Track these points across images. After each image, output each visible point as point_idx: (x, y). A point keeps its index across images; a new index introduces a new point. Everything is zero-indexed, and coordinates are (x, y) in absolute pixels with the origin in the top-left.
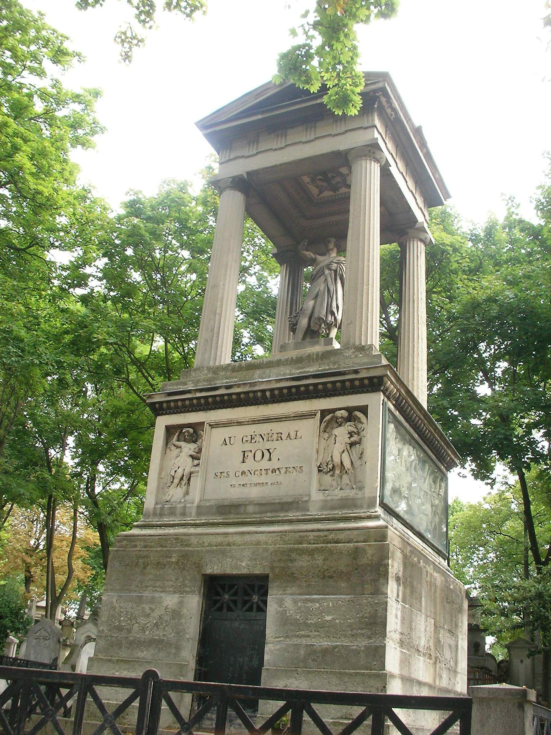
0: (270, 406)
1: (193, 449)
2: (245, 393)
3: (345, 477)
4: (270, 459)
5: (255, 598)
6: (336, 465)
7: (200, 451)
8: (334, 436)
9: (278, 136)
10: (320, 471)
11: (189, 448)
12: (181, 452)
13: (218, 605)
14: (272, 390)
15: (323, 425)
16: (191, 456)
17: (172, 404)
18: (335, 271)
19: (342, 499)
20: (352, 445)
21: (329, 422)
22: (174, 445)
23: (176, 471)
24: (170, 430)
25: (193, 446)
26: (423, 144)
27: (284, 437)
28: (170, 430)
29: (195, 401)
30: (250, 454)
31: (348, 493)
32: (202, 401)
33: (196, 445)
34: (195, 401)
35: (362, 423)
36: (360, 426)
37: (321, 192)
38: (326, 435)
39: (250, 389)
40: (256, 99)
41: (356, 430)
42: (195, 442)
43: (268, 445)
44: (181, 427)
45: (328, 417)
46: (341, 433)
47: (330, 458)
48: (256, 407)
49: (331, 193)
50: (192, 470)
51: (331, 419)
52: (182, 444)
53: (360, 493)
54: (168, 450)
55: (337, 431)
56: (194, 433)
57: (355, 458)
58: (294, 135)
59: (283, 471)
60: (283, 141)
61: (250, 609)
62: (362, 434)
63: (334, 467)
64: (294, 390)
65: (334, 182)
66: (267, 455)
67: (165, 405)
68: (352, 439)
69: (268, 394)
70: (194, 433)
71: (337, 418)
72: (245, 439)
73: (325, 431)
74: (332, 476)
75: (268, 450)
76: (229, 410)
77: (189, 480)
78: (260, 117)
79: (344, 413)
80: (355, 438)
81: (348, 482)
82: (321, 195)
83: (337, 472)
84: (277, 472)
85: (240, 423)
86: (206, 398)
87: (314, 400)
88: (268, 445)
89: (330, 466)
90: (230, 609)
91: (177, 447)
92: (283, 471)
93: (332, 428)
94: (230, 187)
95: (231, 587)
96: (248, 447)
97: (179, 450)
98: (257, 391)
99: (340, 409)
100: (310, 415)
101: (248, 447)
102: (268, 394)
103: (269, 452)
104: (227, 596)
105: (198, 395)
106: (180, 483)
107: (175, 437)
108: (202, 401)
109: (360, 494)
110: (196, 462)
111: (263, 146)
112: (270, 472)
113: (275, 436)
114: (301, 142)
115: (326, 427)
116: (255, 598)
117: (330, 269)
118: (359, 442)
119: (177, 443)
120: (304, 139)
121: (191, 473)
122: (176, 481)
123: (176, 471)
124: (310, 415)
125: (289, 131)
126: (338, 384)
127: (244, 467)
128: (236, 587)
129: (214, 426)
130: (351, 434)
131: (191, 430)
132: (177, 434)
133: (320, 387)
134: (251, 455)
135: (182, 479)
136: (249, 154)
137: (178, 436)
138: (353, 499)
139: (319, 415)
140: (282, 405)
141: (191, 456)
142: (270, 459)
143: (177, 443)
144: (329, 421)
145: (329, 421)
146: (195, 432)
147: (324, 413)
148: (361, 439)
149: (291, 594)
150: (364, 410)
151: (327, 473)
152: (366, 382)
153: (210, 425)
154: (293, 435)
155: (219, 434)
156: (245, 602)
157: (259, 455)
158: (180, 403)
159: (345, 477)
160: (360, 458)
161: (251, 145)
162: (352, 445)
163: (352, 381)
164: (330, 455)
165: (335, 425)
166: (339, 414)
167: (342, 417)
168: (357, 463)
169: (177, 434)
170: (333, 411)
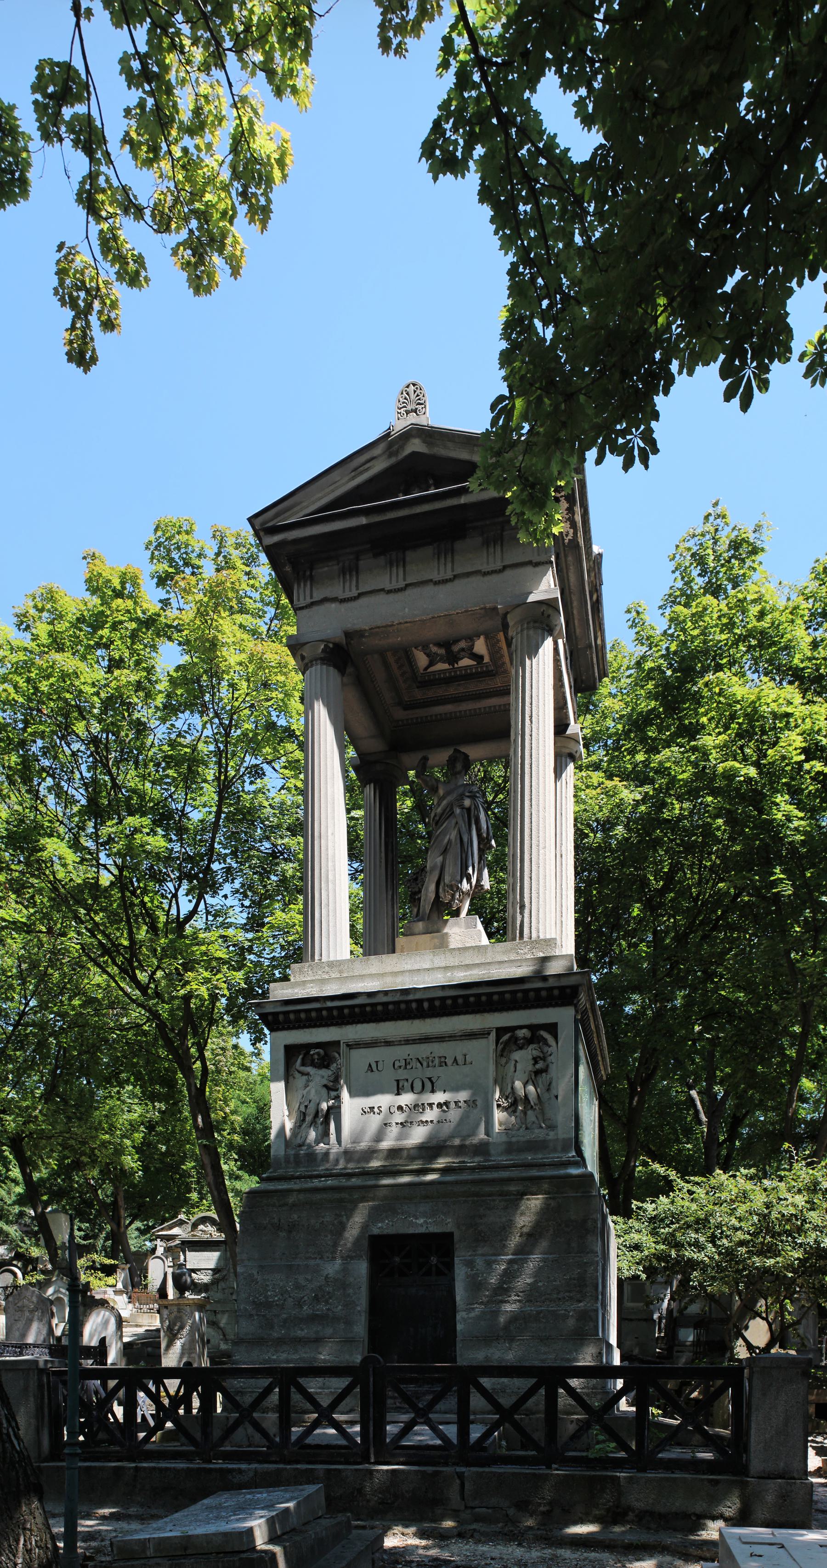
0: (428, 1021)
11: (320, 1076)
12: (308, 1081)
15: (500, 1047)
16: (325, 1086)
19: (529, 1142)
20: (538, 1073)
21: (507, 1043)
22: (299, 1072)
23: (306, 1107)
24: (291, 1052)
25: (325, 1072)
27: (449, 1061)
31: (538, 1134)
32: (335, 1013)
33: (330, 1073)
36: (546, 1049)
38: (504, 1060)
42: (327, 1067)
43: (429, 1073)
44: (308, 1047)
45: (506, 1037)
46: (523, 1057)
47: (509, 1090)
48: (410, 1022)
51: (510, 1038)
52: (309, 1069)
53: (552, 1134)
54: (291, 1079)
55: (517, 1055)
62: (549, 1059)
66: (428, 1085)
67: (281, 1017)
68: (538, 1066)
72: (397, 1064)
73: (502, 1055)
75: (430, 1079)
76: (372, 1025)
81: (534, 1119)
84: (444, 1108)
85: (388, 1043)
87: (486, 1015)
88: (429, 1073)
91: (303, 1074)
93: (511, 1051)
96: (402, 1074)
97: (305, 1077)
99: (521, 1027)
100: (483, 1034)
101: (402, 1074)
107: (299, 1061)
108: (335, 1013)
109: (552, 1135)
111: (369, 582)
112: (435, 1107)
113: (437, 1061)
114: (431, 580)
115: (503, 1050)
118: (545, 1070)
119: (302, 1069)
120: (436, 577)
122: (309, 1119)
123: (306, 1107)
124: (483, 1034)
125: (410, 555)
129: (353, 1045)
130: (536, 1060)
131: (321, 1051)
137: (303, 1059)
138: (544, 1141)
139: (493, 1035)
140: (444, 1020)
141: (325, 1086)
143: (302, 1069)
144: (508, 1041)
145: (508, 1041)
146: (326, 1054)
147: (501, 1031)
148: (547, 1066)
149: (483, 1255)
153: (348, 1045)
154: (460, 1059)
155: (360, 1059)
158: (303, 1016)
161: (348, 577)
162: (538, 1073)
165: (514, 1047)
167: (524, 1038)
170: (512, 1029)
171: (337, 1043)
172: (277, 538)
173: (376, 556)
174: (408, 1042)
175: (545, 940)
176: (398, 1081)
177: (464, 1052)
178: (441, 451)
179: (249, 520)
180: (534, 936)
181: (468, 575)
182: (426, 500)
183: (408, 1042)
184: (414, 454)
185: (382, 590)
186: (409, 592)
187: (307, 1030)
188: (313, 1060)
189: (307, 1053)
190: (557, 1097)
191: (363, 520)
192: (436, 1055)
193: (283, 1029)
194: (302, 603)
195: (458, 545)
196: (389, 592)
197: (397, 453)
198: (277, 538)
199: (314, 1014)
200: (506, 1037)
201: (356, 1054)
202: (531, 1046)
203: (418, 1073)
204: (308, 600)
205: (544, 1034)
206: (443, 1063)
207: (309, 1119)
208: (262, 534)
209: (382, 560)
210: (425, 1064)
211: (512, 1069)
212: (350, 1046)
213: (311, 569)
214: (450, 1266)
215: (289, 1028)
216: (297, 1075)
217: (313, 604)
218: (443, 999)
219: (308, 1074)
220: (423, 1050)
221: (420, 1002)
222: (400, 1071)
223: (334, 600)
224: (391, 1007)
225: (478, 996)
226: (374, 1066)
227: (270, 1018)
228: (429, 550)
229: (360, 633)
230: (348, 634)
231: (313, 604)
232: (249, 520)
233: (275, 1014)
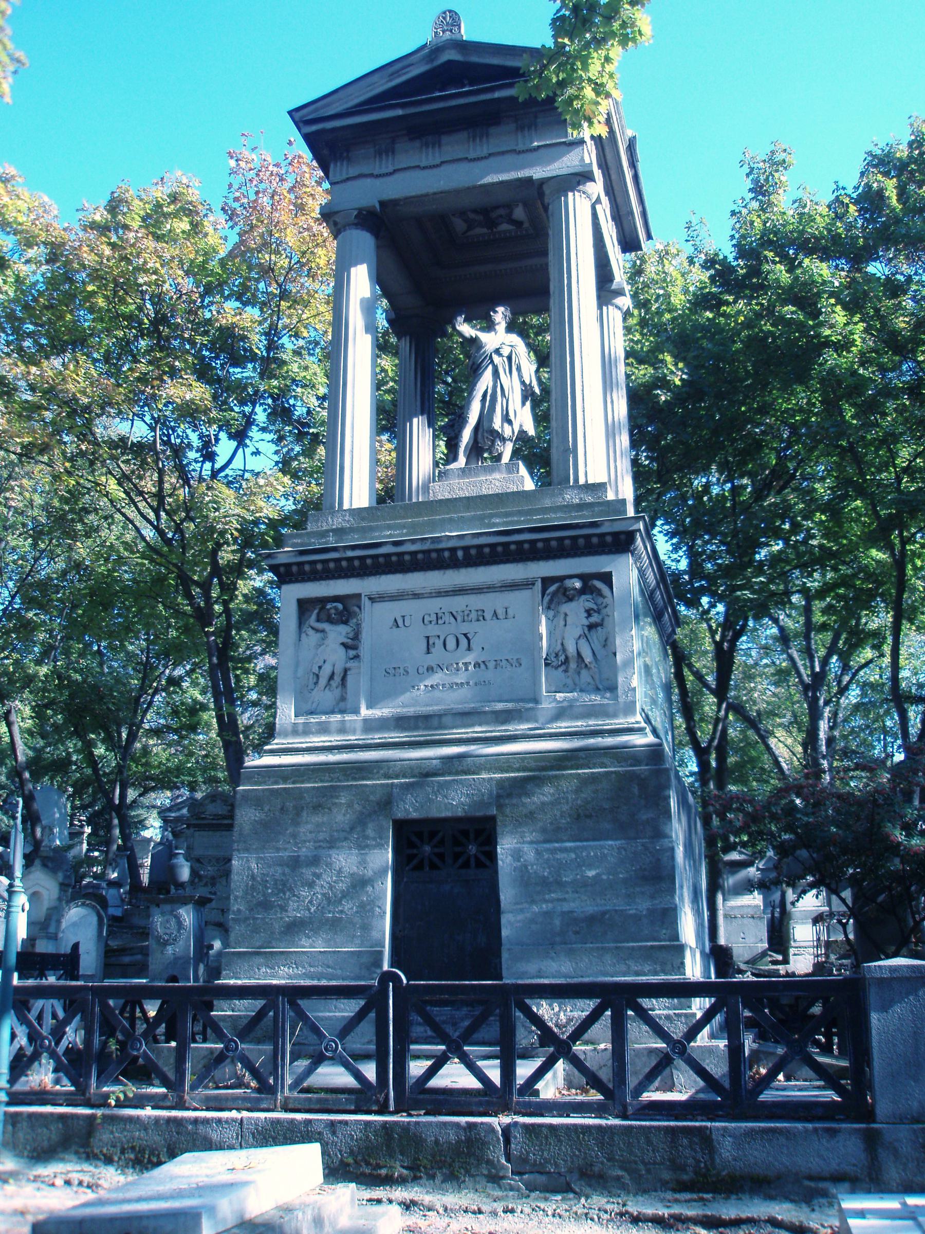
0: (463, 571)
1: (344, 634)
2: (423, 552)
3: (584, 672)
4: (469, 648)
5: (472, 849)
6: (570, 655)
7: (356, 636)
8: (562, 616)
9: (427, 145)
10: (547, 665)
11: (338, 633)
13: (415, 862)
14: (466, 549)
15: (547, 599)
16: (343, 644)
17: (307, 568)
18: (509, 358)
20: (591, 627)
21: (554, 594)
22: (313, 628)
23: (320, 667)
24: (304, 606)
26: (633, 164)
27: (488, 615)
28: (304, 606)
29: (344, 564)
30: (437, 641)
32: (356, 563)
34: (344, 564)
35: (604, 597)
36: (600, 600)
37: (470, 228)
38: (551, 613)
39: (432, 547)
40: (391, 80)
41: (595, 607)
42: (346, 622)
43: (465, 628)
44: (322, 601)
45: (553, 588)
46: (576, 611)
47: (559, 647)
48: (442, 572)
49: (485, 230)
50: (348, 665)
51: (559, 588)
54: (303, 635)
56: (344, 611)
57: (597, 646)
58: (454, 146)
59: (491, 665)
60: (437, 154)
61: (466, 865)
62: (604, 611)
63: (567, 658)
64: (500, 549)
65: (494, 215)
66: (463, 641)
69: (460, 554)
70: (344, 611)
71: (566, 589)
72: (427, 619)
74: (566, 671)
75: (465, 635)
77: (344, 679)
78: (400, 112)
79: (578, 584)
80: (595, 618)
81: (589, 680)
82: (469, 233)
83: (573, 665)
84: (482, 666)
85: (416, 596)
86: (362, 559)
88: (465, 628)
89: (562, 658)
90: (433, 866)
91: (317, 630)
92: (491, 665)
93: (559, 604)
94: (356, 224)
95: (433, 834)
96: (433, 630)
97: (319, 635)
98: (443, 550)
99: (571, 577)
100: (528, 584)
101: (433, 630)
102: (460, 554)
103: (469, 640)
104: (427, 849)
105: (350, 554)
106: (328, 684)
107: (314, 616)
108: (356, 563)
110: (352, 653)
111: (403, 160)
113: (473, 615)
115: (551, 601)
116: (472, 849)
117: (500, 355)
121: (346, 671)
122: (323, 681)
123: (320, 667)
124: (528, 584)
125: (445, 139)
126: (567, 542)
127: (431, 660)
128: (441, 834)
130: (589, 613)
131: (340, 606)
132: (316, 612)
133: (540, 545)
134: (439, 643)
135: (331, 677)
136: (384, 171)
139: (539, 585)
141: (343, 644)
142: (469, 648)
146: (345, 608)
147: (547, 582)
148: (603, 620)
150: (607, 578)
151: (557, 668)
152: (609, 539)
156: (457, 856)
157: (451, 643)
159: (584, 672)
160: (604, 646)
162: (591, 627)
163: (588, 537)
164: (559, 642)
166: (569, 583)
168: (600, 653)
169: (316, 612)
170: (561, 579)
171: (359, 596)
172: (314, 128)
173: (411, 140)
174: (440, 594)
175: (593, 485)
176: (428, 637)
177: (506, 605)
178: (475, 59)
179: (290, 113)
180: (582, 481)
181: (503, 153)
182: (462, 97)
183: (440, 594)
184: (449, 62)
185: (418, 167)
186: (443, 168)
187: (323, 582)
188: (329, 616)
189: (322, 608)
190: (615, 654)
191: (400, 112)
192: (473, 608)
193: (297, 581)
194: (338, 179)
195: (492, 130)
196: (425, 168)
197: (432, 61)
198: (314, 128)
199: (332, 565)
200: (553, 588)
201: (378, 606)
202: (583, 597)
203: (451, 628)
204: (344, 176)
205: (598, 584)
206: (481, 616)
207: (323, 681)
208: (301, 125)
209: (417, 144)
210: (459, 619)
211: (562, 623)
212: (372, 599)
213: (348, 151)
214: (492, 856)
215: (303, 580)
216: (311, 632)
217: (348, 179)
218: (480, 547)
219: (323, 631)
220: (458, 603)
221: (453, 550)
222: (430, 627)
223: (371, 175)
224: (420, 556)
225: (519, 543)
226: (400, 622)
227: (282, 569)
228: (463, 135)
229: (394, 203)
230: (382, 204)
231: (348, 179)
232: (290, 113)
233: (288, 566)
